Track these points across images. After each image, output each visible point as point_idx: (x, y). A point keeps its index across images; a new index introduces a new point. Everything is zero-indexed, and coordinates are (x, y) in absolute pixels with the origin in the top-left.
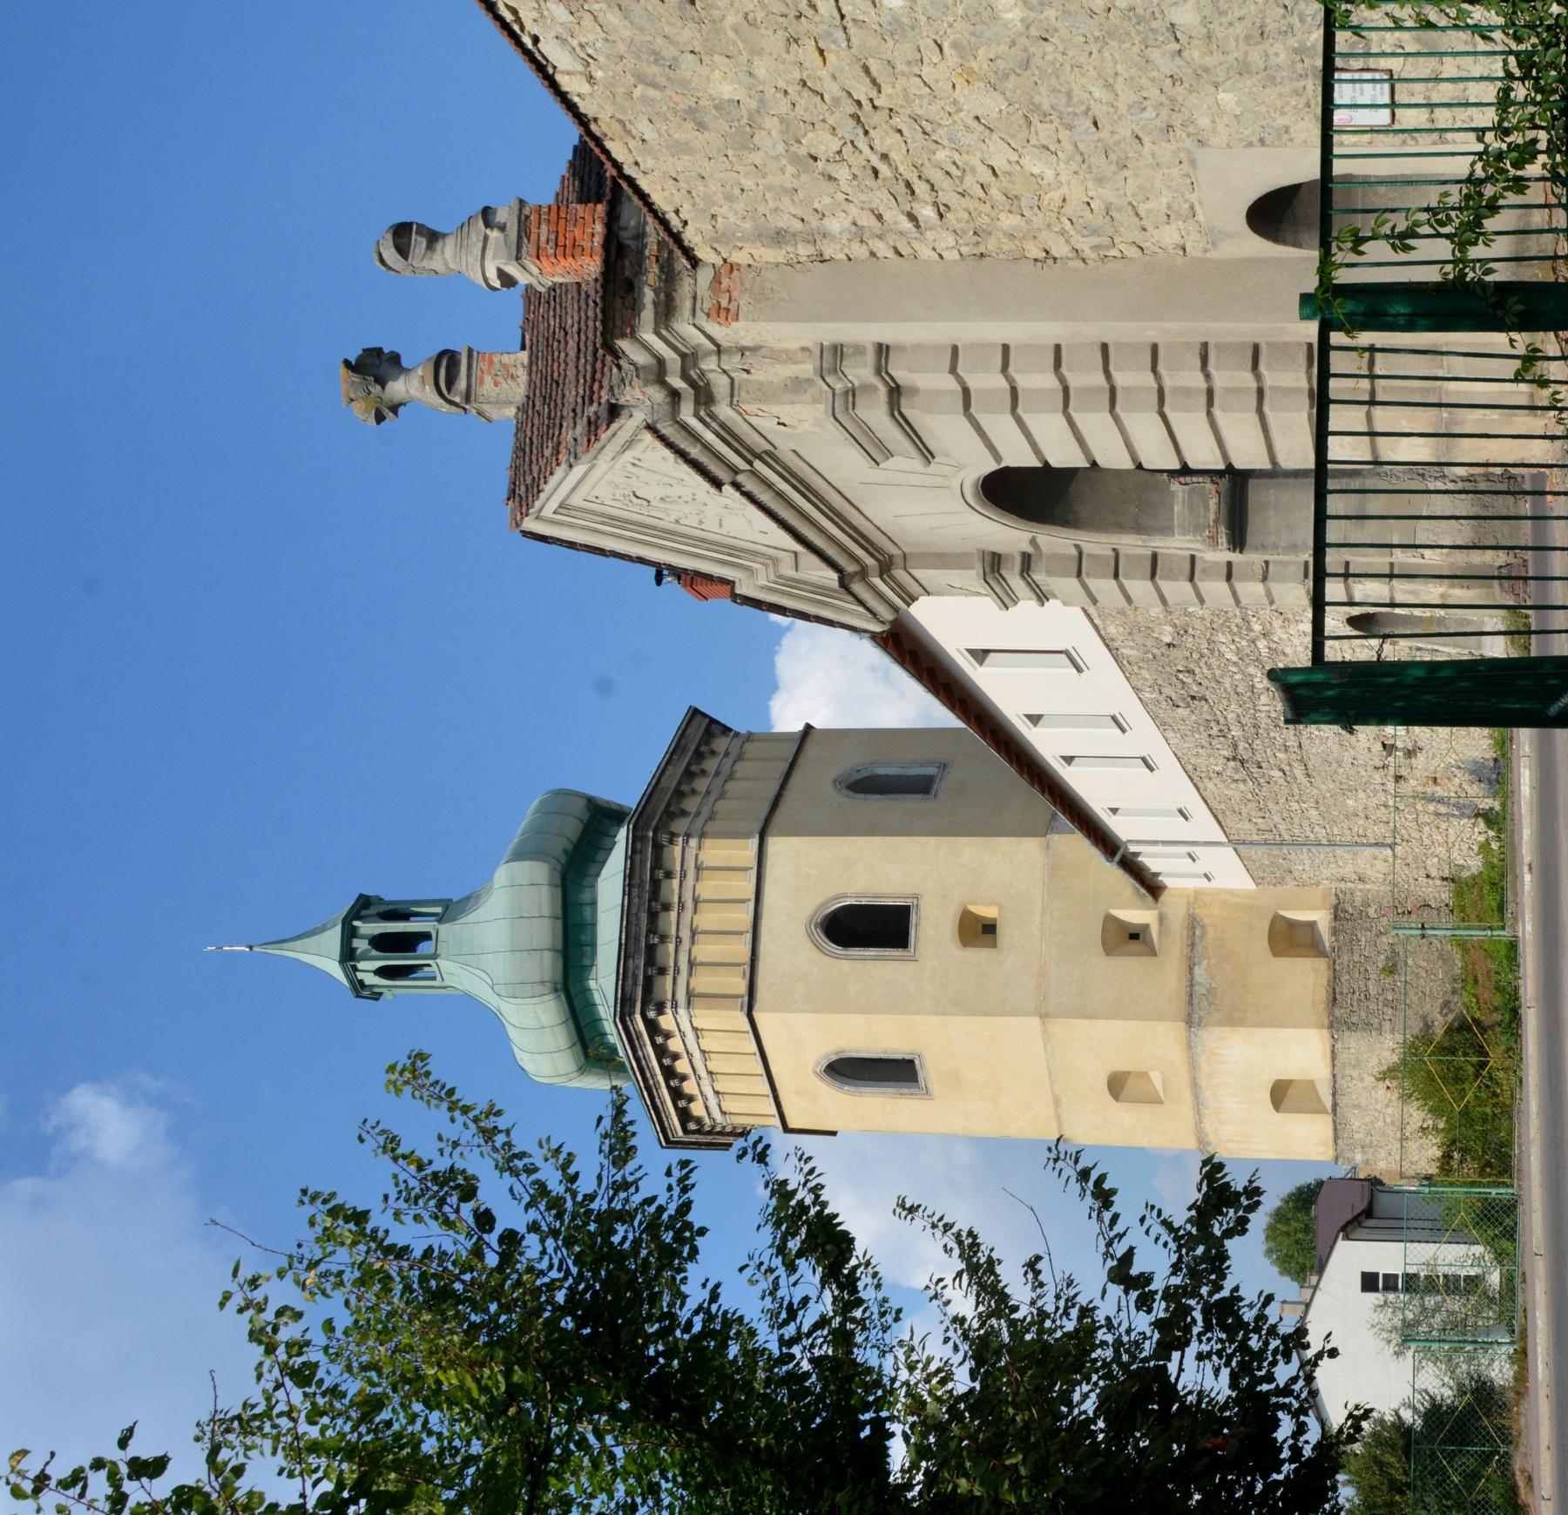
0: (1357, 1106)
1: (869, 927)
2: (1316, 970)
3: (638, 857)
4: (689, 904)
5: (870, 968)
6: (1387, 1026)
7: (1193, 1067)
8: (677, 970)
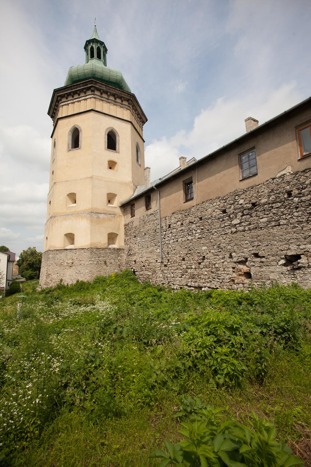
0: (67, 255)
1: (112, 142)
2: (105, 244)
8: (102, 97)
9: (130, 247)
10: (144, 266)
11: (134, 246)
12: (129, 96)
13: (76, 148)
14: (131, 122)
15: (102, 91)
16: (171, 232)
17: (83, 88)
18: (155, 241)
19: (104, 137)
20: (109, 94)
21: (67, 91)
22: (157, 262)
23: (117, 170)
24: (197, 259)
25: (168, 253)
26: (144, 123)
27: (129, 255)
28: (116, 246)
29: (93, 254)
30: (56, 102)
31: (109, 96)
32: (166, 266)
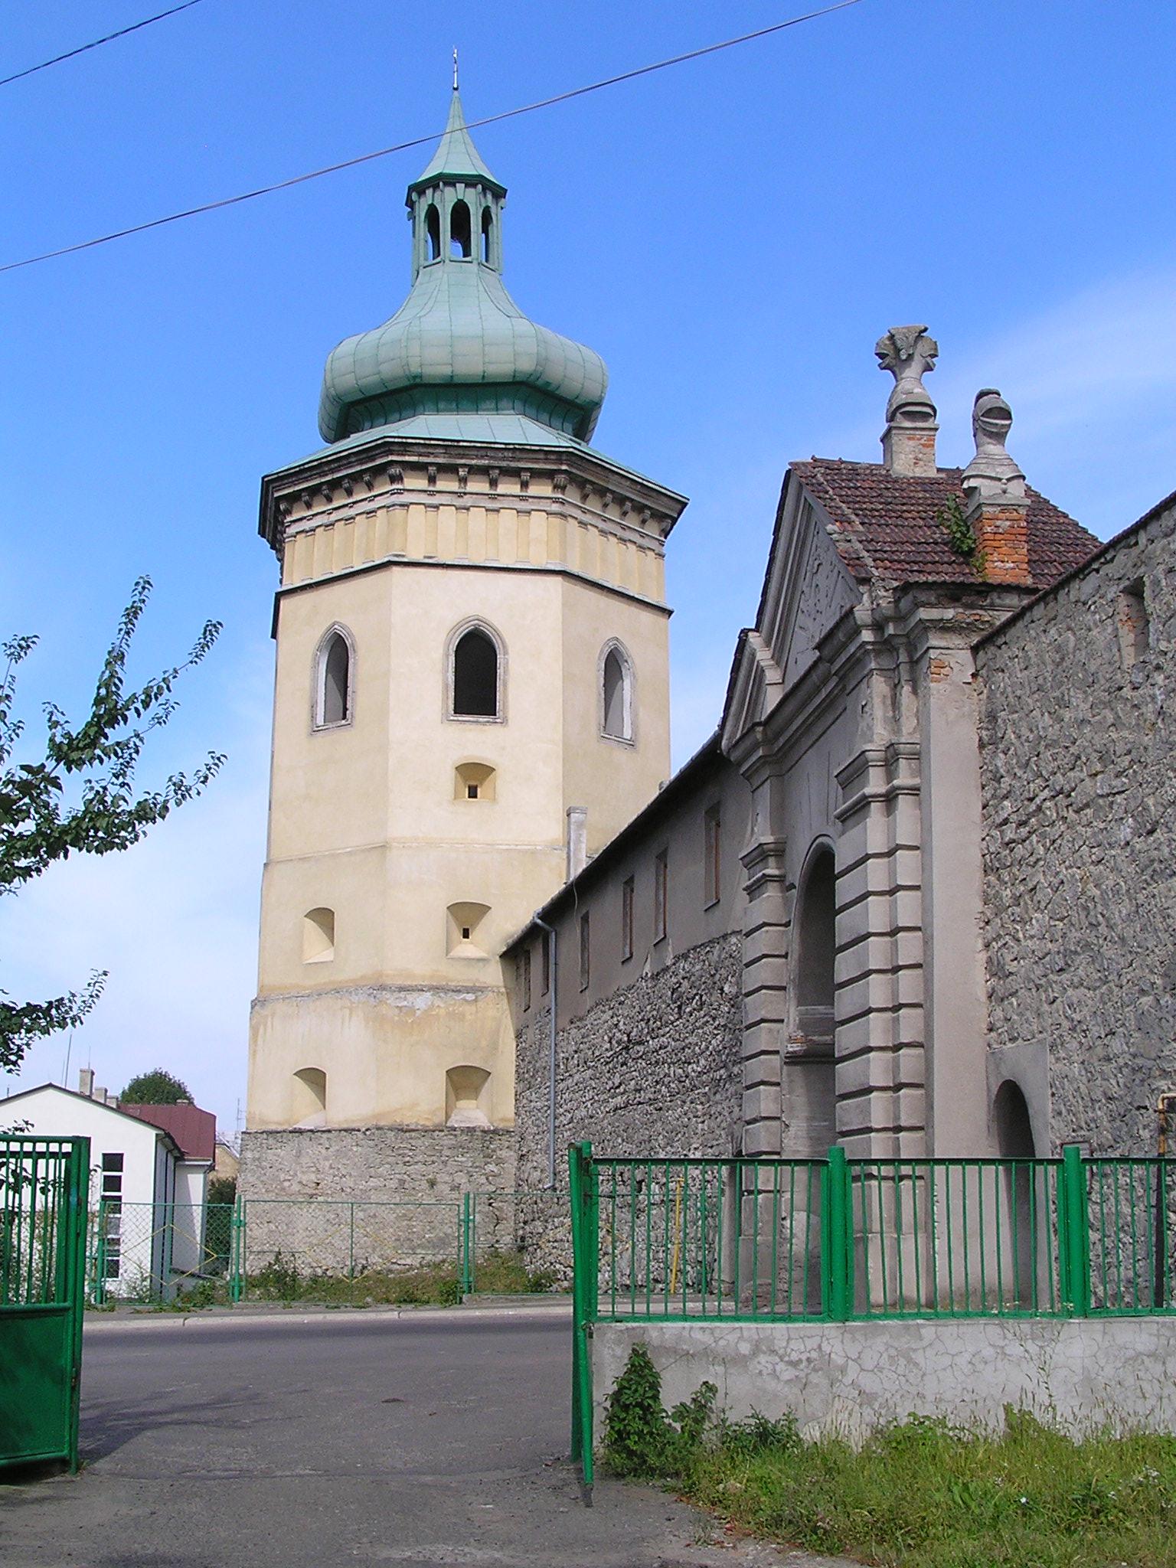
0: (299, 1155)
1: (476, 675)
3: (542, 456)
5: (433, 675)
7: (338, 990)
8: (432, 493)
17: (358, 468)
19: (439, 666)
21: (306, 480)
31: (463, 481)
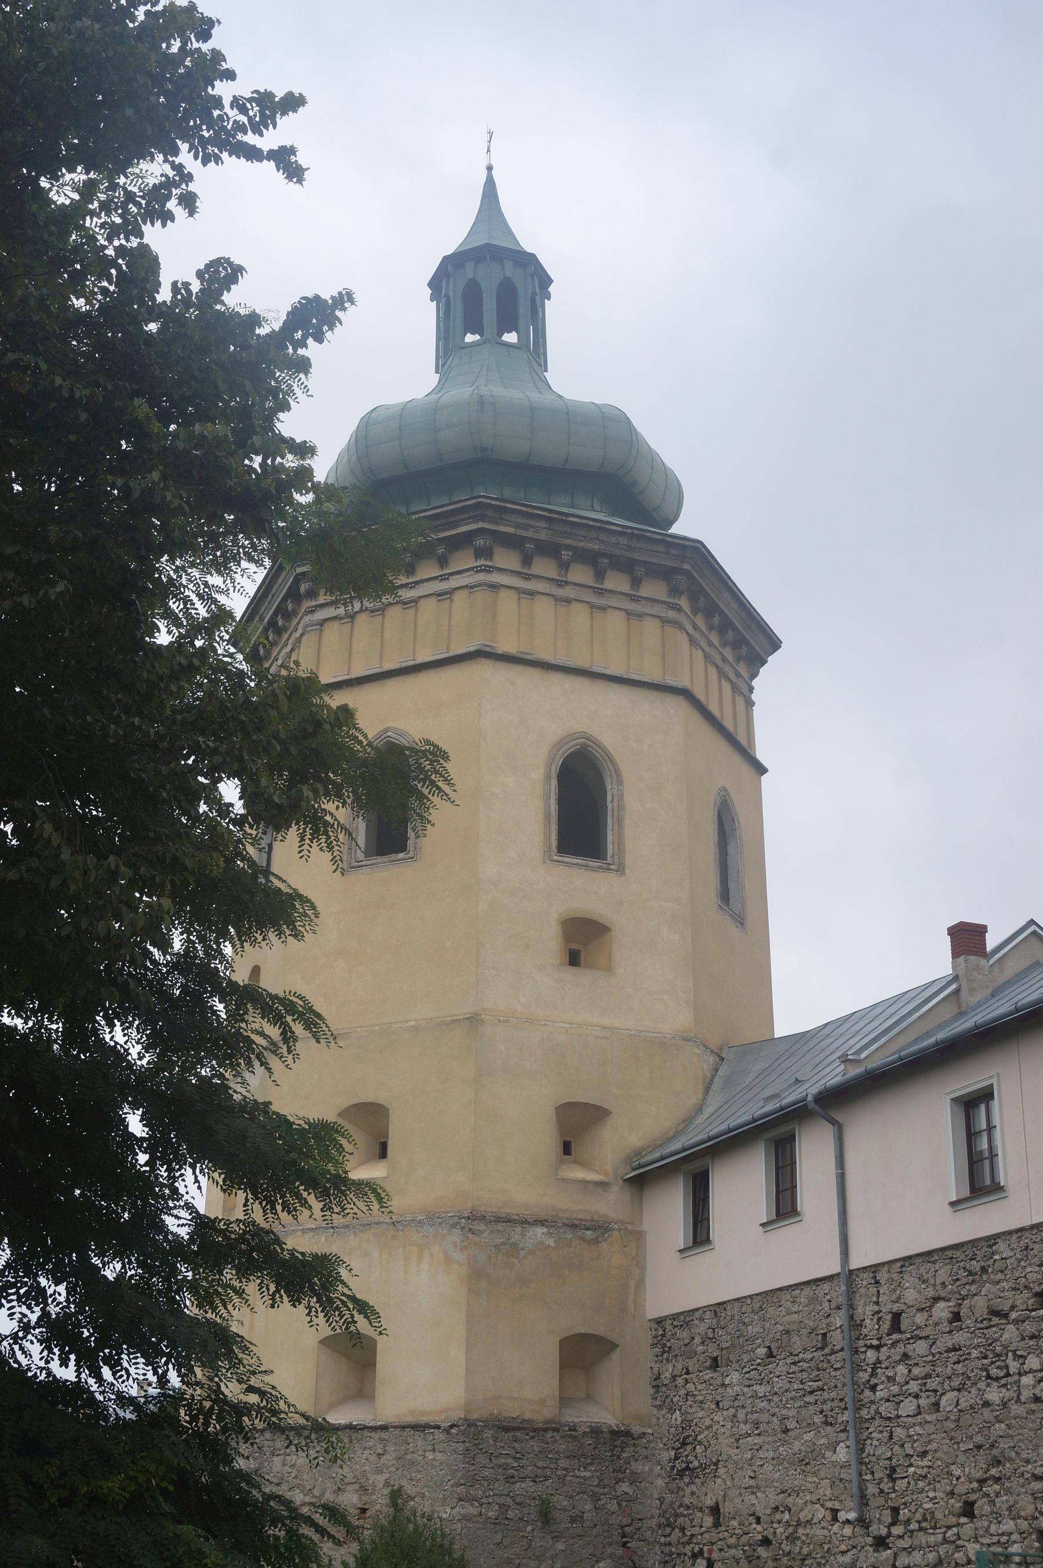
1: (582, 810)
2: (543, 1402)
3: (662, 549)
4: (603, 602)
6: (471, 1510)
8: (527, 577)
9: (687, 1423)
10: (766, 1542)
11: (708, 1422)
12: (675, 552)
13: (393, 857)
14: (686, 694)
15: (530, 546)
16: (906, 1356)
18: (826, 1395)
20: (565, 555)
22: (835, 1519)
23: (609, 969)
24: (1030, 1509)
25: (893, 1470)
26: (756, 661)
27: (681, 1473)
28: (604, 1414)
29: (483, 1460)
30: (285, 599)
31: (564, 566)
32: (881, 1543)
